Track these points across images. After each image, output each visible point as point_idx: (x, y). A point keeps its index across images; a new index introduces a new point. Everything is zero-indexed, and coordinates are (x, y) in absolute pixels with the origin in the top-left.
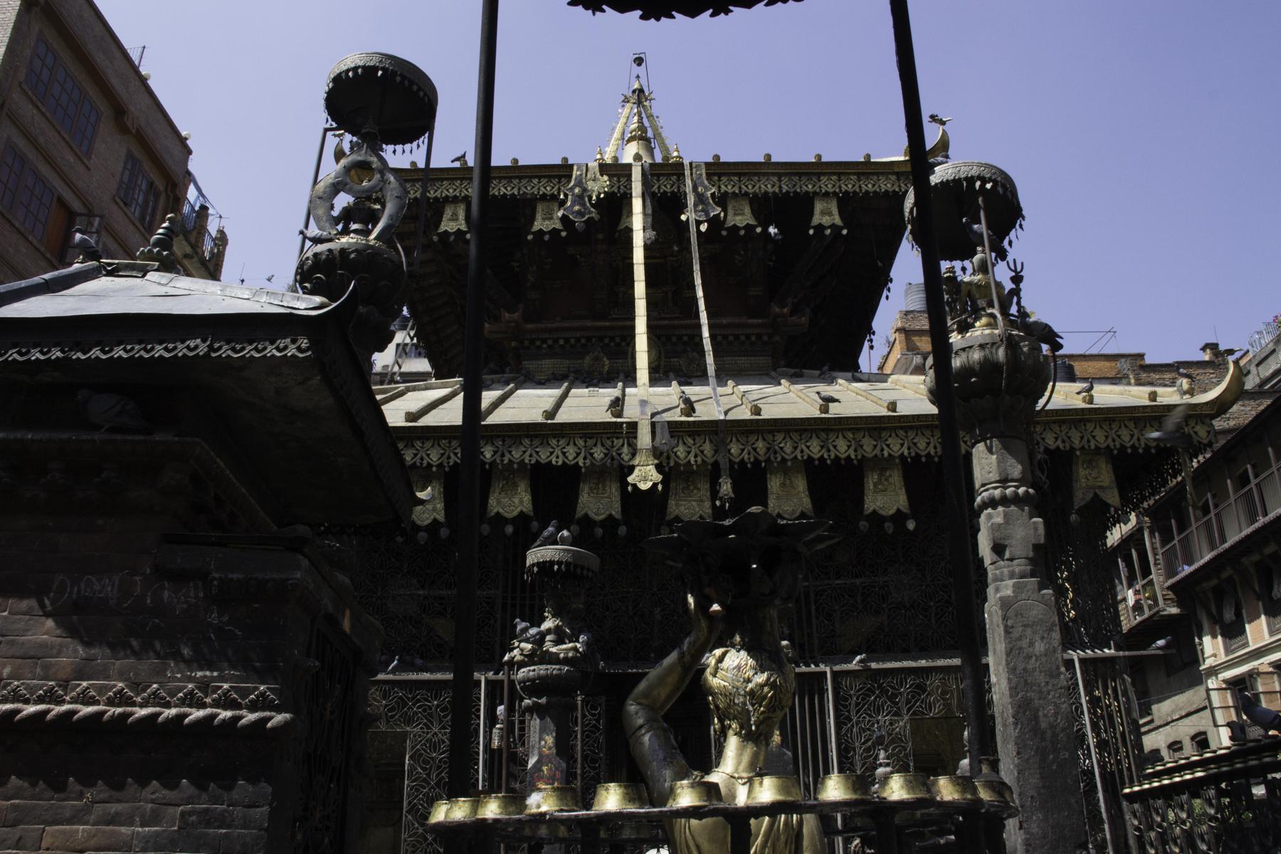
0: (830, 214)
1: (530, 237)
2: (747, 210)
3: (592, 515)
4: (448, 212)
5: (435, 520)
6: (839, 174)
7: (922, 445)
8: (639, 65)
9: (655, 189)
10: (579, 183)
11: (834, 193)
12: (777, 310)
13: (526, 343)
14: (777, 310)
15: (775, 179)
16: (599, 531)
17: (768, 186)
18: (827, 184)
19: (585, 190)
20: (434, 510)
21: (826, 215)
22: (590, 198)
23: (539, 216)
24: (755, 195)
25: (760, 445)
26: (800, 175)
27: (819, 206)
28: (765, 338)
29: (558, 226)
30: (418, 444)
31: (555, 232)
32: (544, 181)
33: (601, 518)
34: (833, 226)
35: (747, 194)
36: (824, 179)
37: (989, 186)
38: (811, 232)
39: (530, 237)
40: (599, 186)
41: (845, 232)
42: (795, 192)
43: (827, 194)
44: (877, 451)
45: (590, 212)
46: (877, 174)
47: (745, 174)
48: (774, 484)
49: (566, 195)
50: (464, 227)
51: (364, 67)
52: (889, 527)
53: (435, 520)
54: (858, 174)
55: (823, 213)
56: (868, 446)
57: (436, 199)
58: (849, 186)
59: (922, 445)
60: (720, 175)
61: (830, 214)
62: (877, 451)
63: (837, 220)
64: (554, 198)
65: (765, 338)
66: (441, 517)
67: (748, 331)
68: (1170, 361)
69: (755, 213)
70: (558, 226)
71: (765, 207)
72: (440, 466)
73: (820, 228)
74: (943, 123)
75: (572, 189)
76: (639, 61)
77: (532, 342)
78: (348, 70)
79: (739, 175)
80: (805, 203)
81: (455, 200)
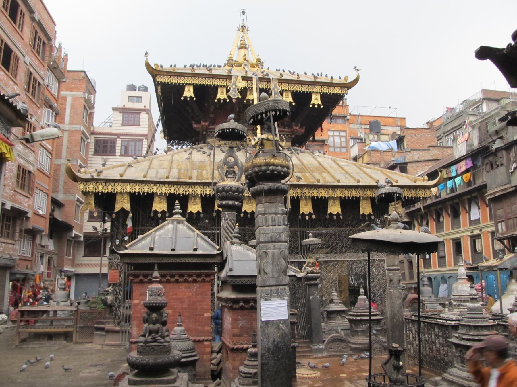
0: (317, 100)
1: (216, 101)
2: (290, 96)
3: (247, 211)
4: (186, 89)
5: (198, 211)
6: (322, 86)
7: (346, 194)
8: (244, 14)
9: (260, 86)
10: (234, 84)
11: (320, 93)
12: (295, 128)
13: (209, 133)
14: (295, 128)
15: (300, 85)
16: (249, 216)
17: (298, 88)
18: (318, 89)
19: (236, 86)
20: (198, 207)
21: (316, 100)
22: (238, 89)
23: (219, 93)
24: (293, 91)
25: (299, 191)
26: (308, 85)
27: (314, 96)
28: (289, 136)
29: (226, 98)
30: (193, 187)
31: (225, 100)
32: (221, 80)
33: (250, 211)
34: (318, 105)
35: (290, 90)
36: (317, 87)
37: (398, 195)
38: (311, 106)
39: (216, 101)
40: (242, 84)
41: (322, 107)
42: (307, 92)
43: (317, 93)
44: (333, 195)
45: (238, 95)
46: (334, 86)
47: (290, 83)
48: (302, 203)
49: (230, 88)
50: (193, 96)
51: (232, 129)
52: (335, 217)
53: (198, 211)
54: (328, 86)
55: (315, 99)
56: (331, 191)
57: (183, 84)
58: (325, 90)
59: (346, 194)
60: (282, 83)
61: (317, 100)
62: (333, 195)
63: (320, 103)
64: (224, 86)
65: (289, 136)
66: (201, 211)
67: (284, 133)
68: (415, 127)
69: (293, 98)
70: (226, 98)
71: (295, 95)
72: (201, 195)
73: (314, 105)
74: (358, 70)
75: (232, 86)
76: (243, 13)
77: (211, 132)
78: (227, 129)
79: (288, 83)
80: (309, 96)
81: (190, 84)
